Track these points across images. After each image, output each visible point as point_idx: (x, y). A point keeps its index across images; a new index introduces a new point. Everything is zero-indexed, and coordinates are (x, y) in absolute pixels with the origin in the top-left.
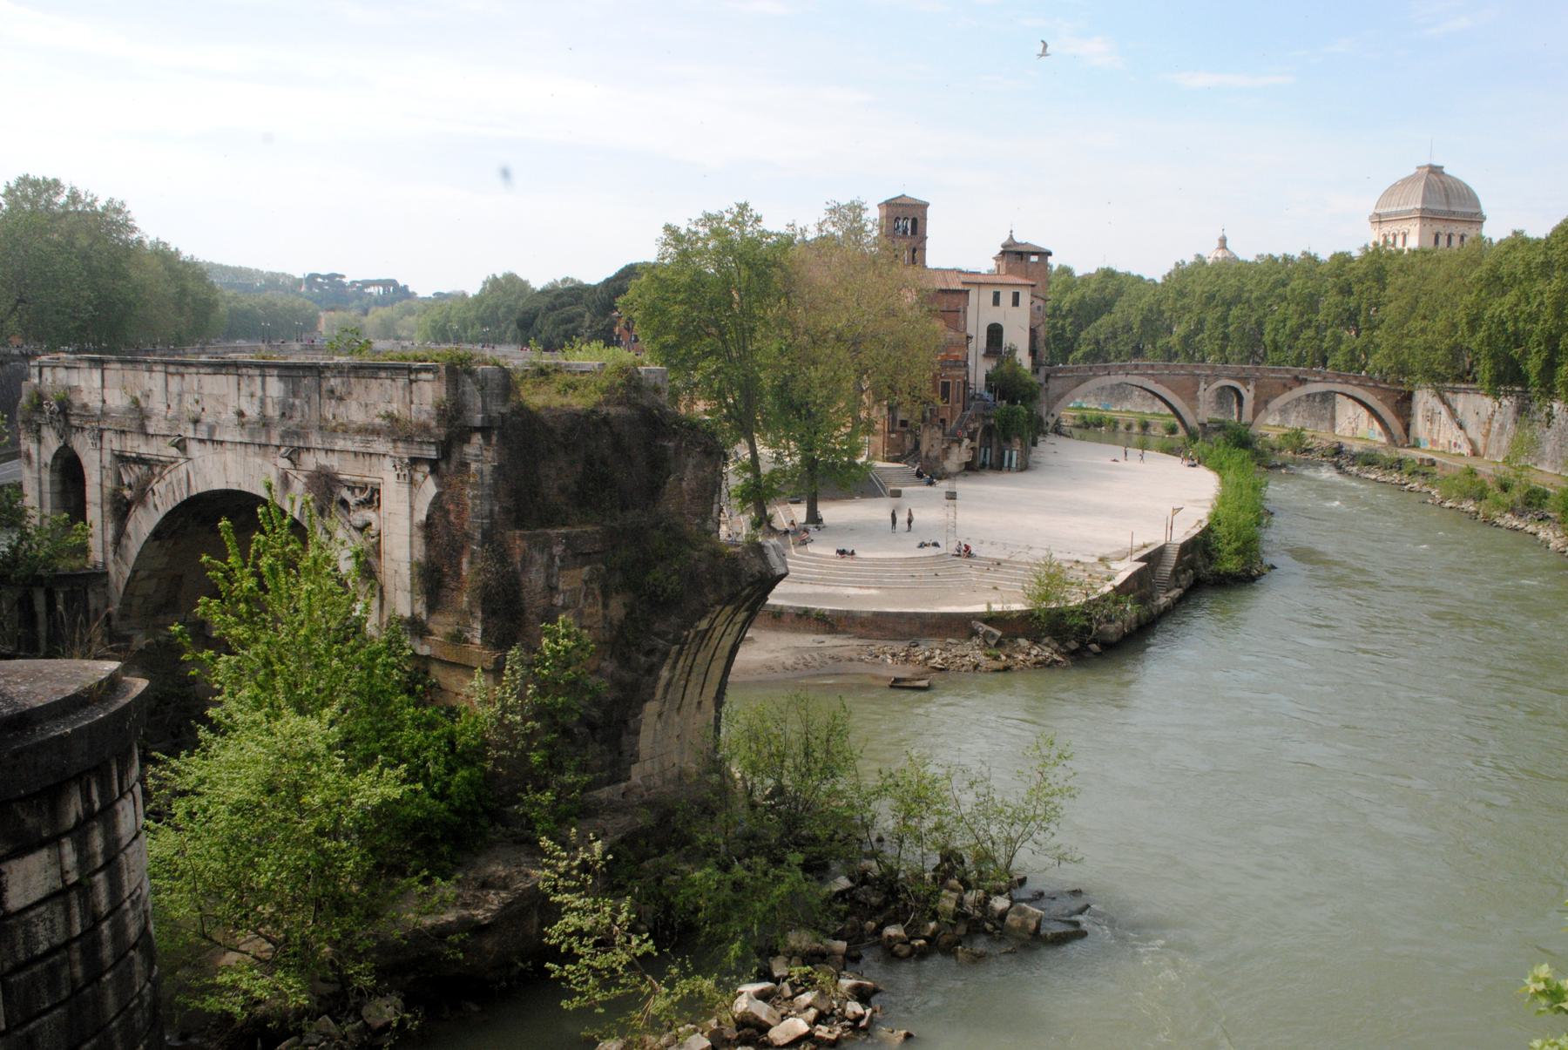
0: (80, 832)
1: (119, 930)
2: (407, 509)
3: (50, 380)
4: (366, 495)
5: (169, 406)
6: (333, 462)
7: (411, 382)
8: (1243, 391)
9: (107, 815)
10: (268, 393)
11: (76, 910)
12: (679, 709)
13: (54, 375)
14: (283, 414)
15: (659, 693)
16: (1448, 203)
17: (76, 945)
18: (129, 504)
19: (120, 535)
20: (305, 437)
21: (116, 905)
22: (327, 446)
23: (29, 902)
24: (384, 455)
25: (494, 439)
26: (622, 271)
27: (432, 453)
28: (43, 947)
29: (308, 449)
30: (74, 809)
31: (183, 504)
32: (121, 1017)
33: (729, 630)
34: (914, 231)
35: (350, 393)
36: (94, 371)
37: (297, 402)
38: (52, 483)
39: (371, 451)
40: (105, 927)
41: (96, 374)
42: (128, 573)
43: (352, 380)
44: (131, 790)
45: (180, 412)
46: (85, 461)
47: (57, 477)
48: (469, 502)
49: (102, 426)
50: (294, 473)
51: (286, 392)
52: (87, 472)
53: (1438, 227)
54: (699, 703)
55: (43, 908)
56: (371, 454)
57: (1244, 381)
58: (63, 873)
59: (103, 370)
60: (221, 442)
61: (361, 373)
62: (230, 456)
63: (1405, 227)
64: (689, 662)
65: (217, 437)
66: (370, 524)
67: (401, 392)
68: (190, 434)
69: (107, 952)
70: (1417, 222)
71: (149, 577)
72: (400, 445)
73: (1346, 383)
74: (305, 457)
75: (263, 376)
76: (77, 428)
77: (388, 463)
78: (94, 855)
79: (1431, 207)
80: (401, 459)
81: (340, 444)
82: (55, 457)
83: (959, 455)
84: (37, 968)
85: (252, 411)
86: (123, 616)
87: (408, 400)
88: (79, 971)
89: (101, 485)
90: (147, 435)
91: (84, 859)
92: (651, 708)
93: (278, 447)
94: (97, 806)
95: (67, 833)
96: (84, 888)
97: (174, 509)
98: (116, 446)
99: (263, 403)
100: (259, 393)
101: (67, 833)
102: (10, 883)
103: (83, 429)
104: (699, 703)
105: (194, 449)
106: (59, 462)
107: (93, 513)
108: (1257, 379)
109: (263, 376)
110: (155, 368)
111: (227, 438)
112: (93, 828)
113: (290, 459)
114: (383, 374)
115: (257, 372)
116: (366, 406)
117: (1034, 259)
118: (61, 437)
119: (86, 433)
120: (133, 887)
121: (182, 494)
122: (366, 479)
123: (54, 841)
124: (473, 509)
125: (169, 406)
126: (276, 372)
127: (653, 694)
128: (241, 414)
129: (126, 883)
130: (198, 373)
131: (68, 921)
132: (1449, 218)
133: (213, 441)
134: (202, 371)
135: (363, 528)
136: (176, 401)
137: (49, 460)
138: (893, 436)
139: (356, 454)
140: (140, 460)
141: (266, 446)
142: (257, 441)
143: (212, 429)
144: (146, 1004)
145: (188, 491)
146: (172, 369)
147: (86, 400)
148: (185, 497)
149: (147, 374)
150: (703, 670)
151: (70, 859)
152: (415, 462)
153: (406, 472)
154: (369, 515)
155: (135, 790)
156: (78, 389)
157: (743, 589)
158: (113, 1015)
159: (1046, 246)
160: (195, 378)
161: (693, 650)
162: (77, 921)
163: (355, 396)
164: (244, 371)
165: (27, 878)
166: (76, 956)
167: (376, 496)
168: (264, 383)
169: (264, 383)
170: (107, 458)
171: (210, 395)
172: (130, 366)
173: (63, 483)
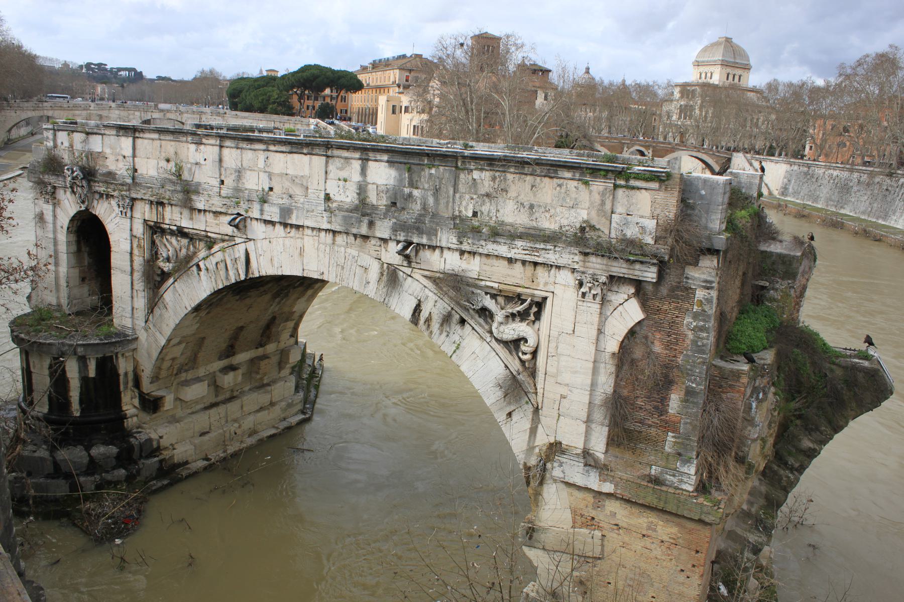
2: (595, 333)
3: (66, 144)
4: (520, 308)
5: (222, 182)
7: (616, 187)
10: (369, 179)
14: (394, 204)
16: (735, 58)
18: (165, 276)
19: (154, 302)
20: (432, 233)
22: (465, 247)
26: (302, 68)
27: (650, 274)
29: (433, 248)
35: (505, 190)
36: (123, 139)
37: (416, 193)
38: (68, 243)
39: (540, 260)
41: (126, 143)
42: (163, 342)
43: (510, 177)
45: (237, 190)
46: (110, 227)
47: (73, 238)
48: (690, 335)
49: (134, 195)
50: (408, 271)
51: (401, 180)
52: (112, 238)
53: (729, 70)
56: (536, 264)
57: (647, 147)
60: (298, 227)
61: (527, 170)
62: (309, 240)
63: (712, 69)
65: (293, 221)
66: (526, 341)
67: (597, 198)
68: (256, 214)
70: (719, 67)
71: (179, 343)
72: (593, 259)
73: (699, 151)
74: (426, 254)
75: (365, 160)
76: (101, 195)
77: (566, 278)
79: (727, 59)
81: (490, 248)
82: (73, 220)
85: (347, 196)
86: (155, 378)
87: (608, 207)
90: (192, 209)
93: (385, 241)
97: (226, 288)
99: (362, 190)
100: (356, 177)
105: (257, 230)
106: (76, 222)
107: (120, 282)
108: (654, 147)
109: (365, 160)
110: (204, 141)
111: (308, 223)
114: (568, 175)
115: (357, 155)
116: (532, 207)
122: (519, 290)
124: (694, 342)
125: (222, 182)
126: (385, 157)
128: (328, 198)
132: (734, 66)
133: (285, 225)
134: (272, 148)
135: (514, 344)
136: (233, 177)
139: (510, 261)
140: (181, 233)
141: (366, 238)
142: (354, 231)
143: (286, 211)
146: (228, 143)
148: (243, 277)
149: (193, 147)
152: (614, 280)
156: (101, 155)
160: (262, 156)
163: (512, 193)
164: (337, 152)
167: (534, 309)
168: (363, 171)
169: (363, 171)
170: (139, 229)
172: (170, 137)
173: (78, 242)
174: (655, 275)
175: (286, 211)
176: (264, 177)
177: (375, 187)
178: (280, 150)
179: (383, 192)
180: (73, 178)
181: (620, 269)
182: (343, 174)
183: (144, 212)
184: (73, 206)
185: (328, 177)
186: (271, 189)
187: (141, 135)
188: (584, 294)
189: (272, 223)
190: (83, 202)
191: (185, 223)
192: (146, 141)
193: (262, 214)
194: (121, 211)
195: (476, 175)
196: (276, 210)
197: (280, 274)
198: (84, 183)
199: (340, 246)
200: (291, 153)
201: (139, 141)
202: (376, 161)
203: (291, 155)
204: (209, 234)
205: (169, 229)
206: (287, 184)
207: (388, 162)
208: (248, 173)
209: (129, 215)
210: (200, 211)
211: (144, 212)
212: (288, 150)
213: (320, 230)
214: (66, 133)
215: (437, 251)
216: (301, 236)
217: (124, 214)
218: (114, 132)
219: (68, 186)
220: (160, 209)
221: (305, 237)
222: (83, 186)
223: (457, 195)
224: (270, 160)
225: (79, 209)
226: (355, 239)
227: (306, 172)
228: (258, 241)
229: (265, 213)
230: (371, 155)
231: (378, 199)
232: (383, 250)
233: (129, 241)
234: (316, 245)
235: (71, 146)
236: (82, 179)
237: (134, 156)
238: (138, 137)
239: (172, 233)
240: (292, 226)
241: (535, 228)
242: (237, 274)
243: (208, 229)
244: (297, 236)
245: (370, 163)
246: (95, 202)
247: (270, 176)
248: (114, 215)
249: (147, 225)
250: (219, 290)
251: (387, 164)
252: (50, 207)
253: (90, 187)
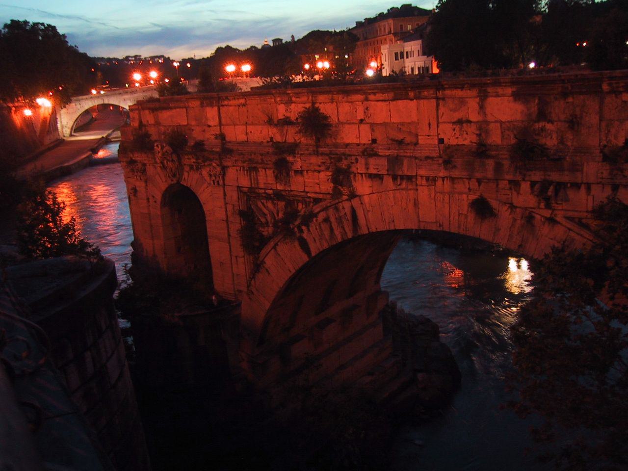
29: (576, 186)
31: (345, 243)
60: (409, 178)
65: (406, 171)
89: (227, 221)
98: (245, 182)
115: (474, 92)
118: (174, 175)
137: (159, 197)
142: (478, 175)
148: (350, 235)
168: (482, 107)
170: (233, 195)
171: (385, 124)
175: (394, 161)
176: (365, 128)
177: (499, 125)
178: (381, 98)
179: (508, 130)
180: (163, 154)
183: (237, 177)
185: (440, 121)
186: (374, 141)
187: (226, 103)
189: (380, 177)
190: (174, 175)
192: (231, 108)
193: (367, 169)
194: (213, 181)
196: (384, 162)
197: (392, 228)
198: (174, 157)
199: (461, 193)
201: (223, 110)
202: (498, 96)
203: (395, 102)
204: (309, 194)
205: (265, 193)
208: (347, 126)
209: (221, 182)
211: (237, 177)
212: (390, 98)
215: (583, 190)
216: (414, 187)
217: (216, 184)
219: (158, 162)
220: (253, 174)
221: (420, 188)
222: (173, 161)
223: (603, 124)
224: (371, 111)
225: (170, 182)
226: (479, 185)
227: (415, 119)
228: (365, 197)
229: (371, 167)
230: (489, 90)
231: (503, 137)
232: (515, 194)
233: (224, 209)
234: (433, 195)
236: (172, 153)
238: (223, 106)
239: (268, 197)
240: (402, 178)
243: (307, 189)
244: (410, 187)
246: (186, 174)
247: (372, 126)
248: (206, 185)
249: (241, 191)
250: (324, 251)
251: (511, 98)
252: (144, 184)
253: (179, 159)
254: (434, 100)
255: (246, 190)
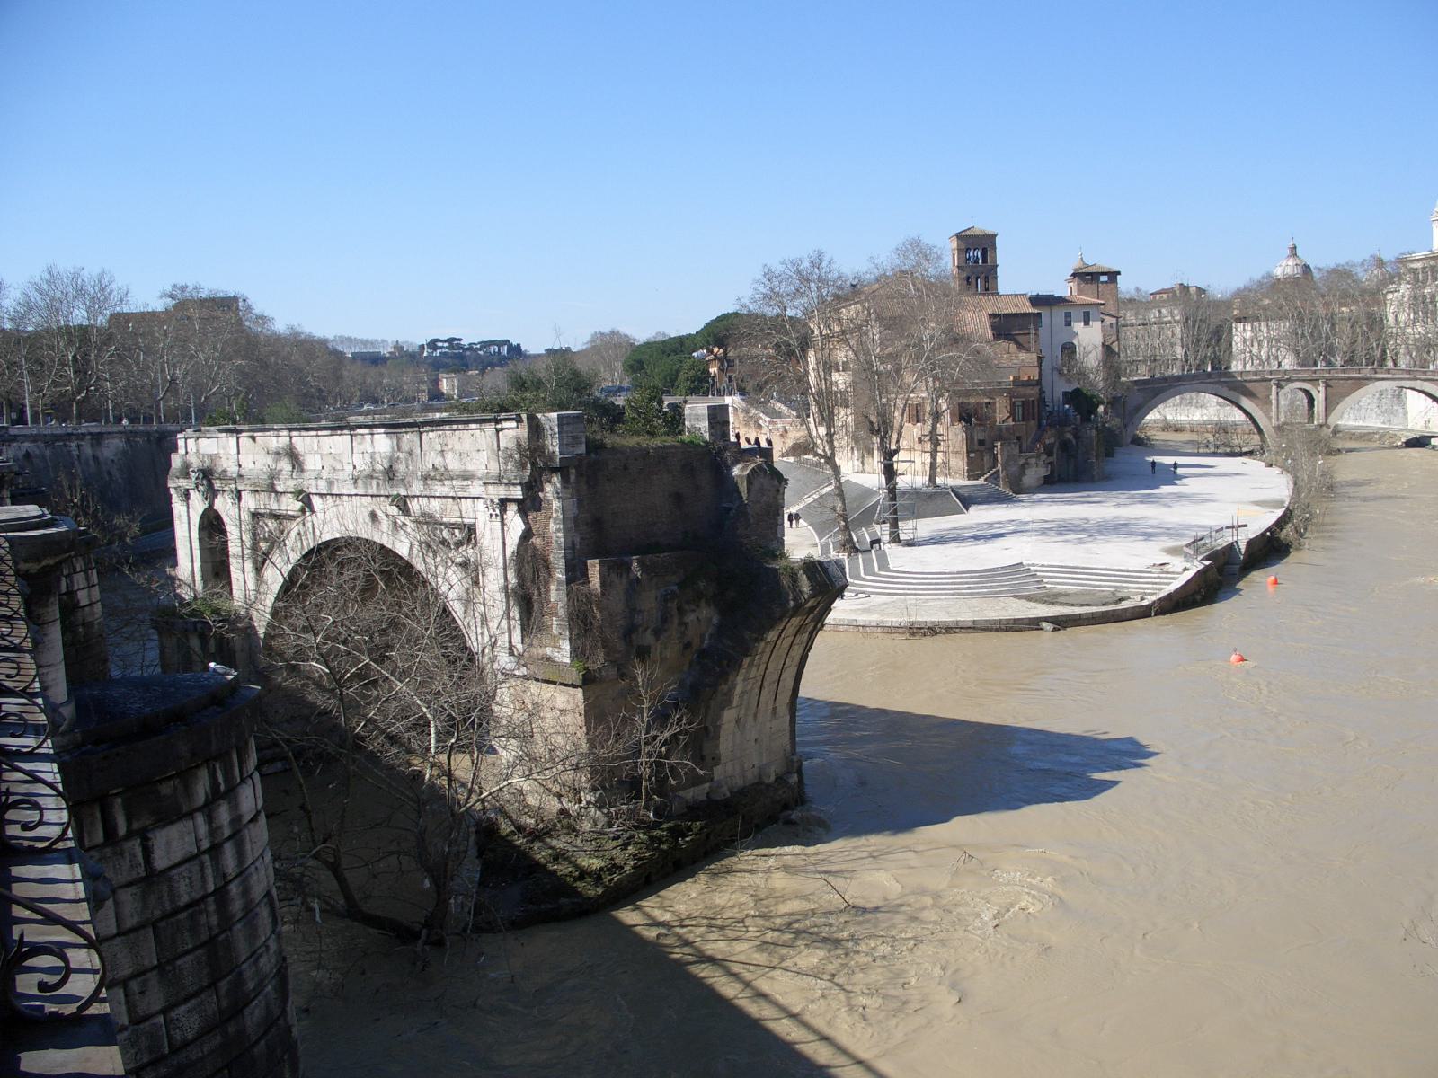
0: (208, 808)
1: (246, 892)
3: (194, 450)
6: (434, 506)
8: (1314, 393)
9: (231, 793)
11: (209, 871)
12: (755, 716)
13: (197, 445)
15: (736, 701)
17: (211, 899)
21: (242, 873)
23: (172, 863)
24: (478, 498)
25: (572, 478)
27: (518, 493)
28: (184, 900)
30: (201, 789)
32: (252, 960)
33: (797, 641)
34: (985, 261)
37: (401, 455)
39: (466, 495)
40: (234, 889)
41: (233, 441)
44: (250, 776)
49: (240, 488)
51: (393, 448)
54: (775, 709)
55: (182, 868)
56: (466, 498)
58: (198, 840)
59: (238, 438)
60: (339, 495)
64: (761, 671)
69: (237, 906)
77: (480, 504)
78: (220, 828)
80: (492, 501)
81: (440, 489)
83: (1035, 473)
84: (182, 916)
88: (214, 920)
90: (276, 492)
91: (213, 831)
92: (729, 715)
94: (222, 787)
95: (199, 809)
96: (215, 850)
99: (372, 455)
101: (199, 809)
102: (155, 847)
103: (224, 491)
104: (775, 709)
111: (345, 492)
112: (219, 805)
113: (398, 506)
114: (473, 426)
115: (367, 431)
117: (1104, 278)
119: (226, 495)
120: (256, 855)
121: (309, 544)
123: (190, 815)
126: (382, 430)
127: (730, 702)
129: (249, 852)
130: (317, 436)
131: (203, 878)
134: (320, 433)
138: (972, 455)
142: (370, 492)
144: (271, 951)
145: (314, 541)
147: (225, 466)
150: (775, 677)
151: (203, 829)
152: (504, 503)
153: (498, 512)
154: (469, 552)
155: (253, 777)
157: (807, 601)
158: (243, 958)
159: (1115, 268)
161: (765, 658)
162: (210, 879)
165: (168, 843)
166: (212, 908)
170: (246, 517)
174: (521, 493)
175: (330, 483)
176: (318, 457)
181: (502, 492)
182: (361, 448)
184: (201, 503)
186: (323, 467)
188: (491, 515)
191: (275, 507)
195: (431, 435)
200: (331, 435)
206: (331, 461)
207: (386, 433)
210: (281, 493)
213: (351, 495)
214: (193, 440)
218: (224, 435)
220: (257, 496)
235: (198, 451)
237: (239, 453)
241: (465, 471)
242: (309, 544)
243: (289, 508)
245: (375, 436)
247: (322, 455)
251: (384, 435)
254: (349, 436)
255: (252, 510)
